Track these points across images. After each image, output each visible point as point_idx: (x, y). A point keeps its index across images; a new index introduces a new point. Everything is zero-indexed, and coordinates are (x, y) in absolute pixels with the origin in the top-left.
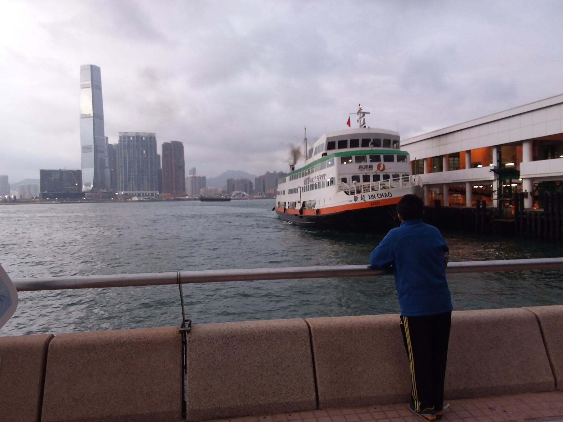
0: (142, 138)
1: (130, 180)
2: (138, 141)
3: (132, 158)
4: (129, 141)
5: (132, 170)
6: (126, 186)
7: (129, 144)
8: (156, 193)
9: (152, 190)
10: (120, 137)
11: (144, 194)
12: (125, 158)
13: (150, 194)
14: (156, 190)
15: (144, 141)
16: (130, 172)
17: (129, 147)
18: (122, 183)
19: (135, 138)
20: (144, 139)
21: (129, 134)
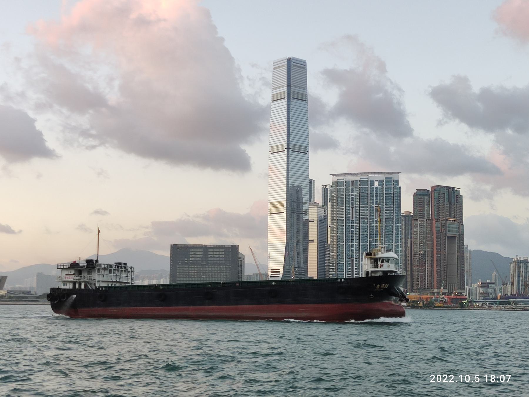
0: (372, 183)
2: (364, 189)
3: (352, 222)
15: (376, 188)
20: (376, 184)
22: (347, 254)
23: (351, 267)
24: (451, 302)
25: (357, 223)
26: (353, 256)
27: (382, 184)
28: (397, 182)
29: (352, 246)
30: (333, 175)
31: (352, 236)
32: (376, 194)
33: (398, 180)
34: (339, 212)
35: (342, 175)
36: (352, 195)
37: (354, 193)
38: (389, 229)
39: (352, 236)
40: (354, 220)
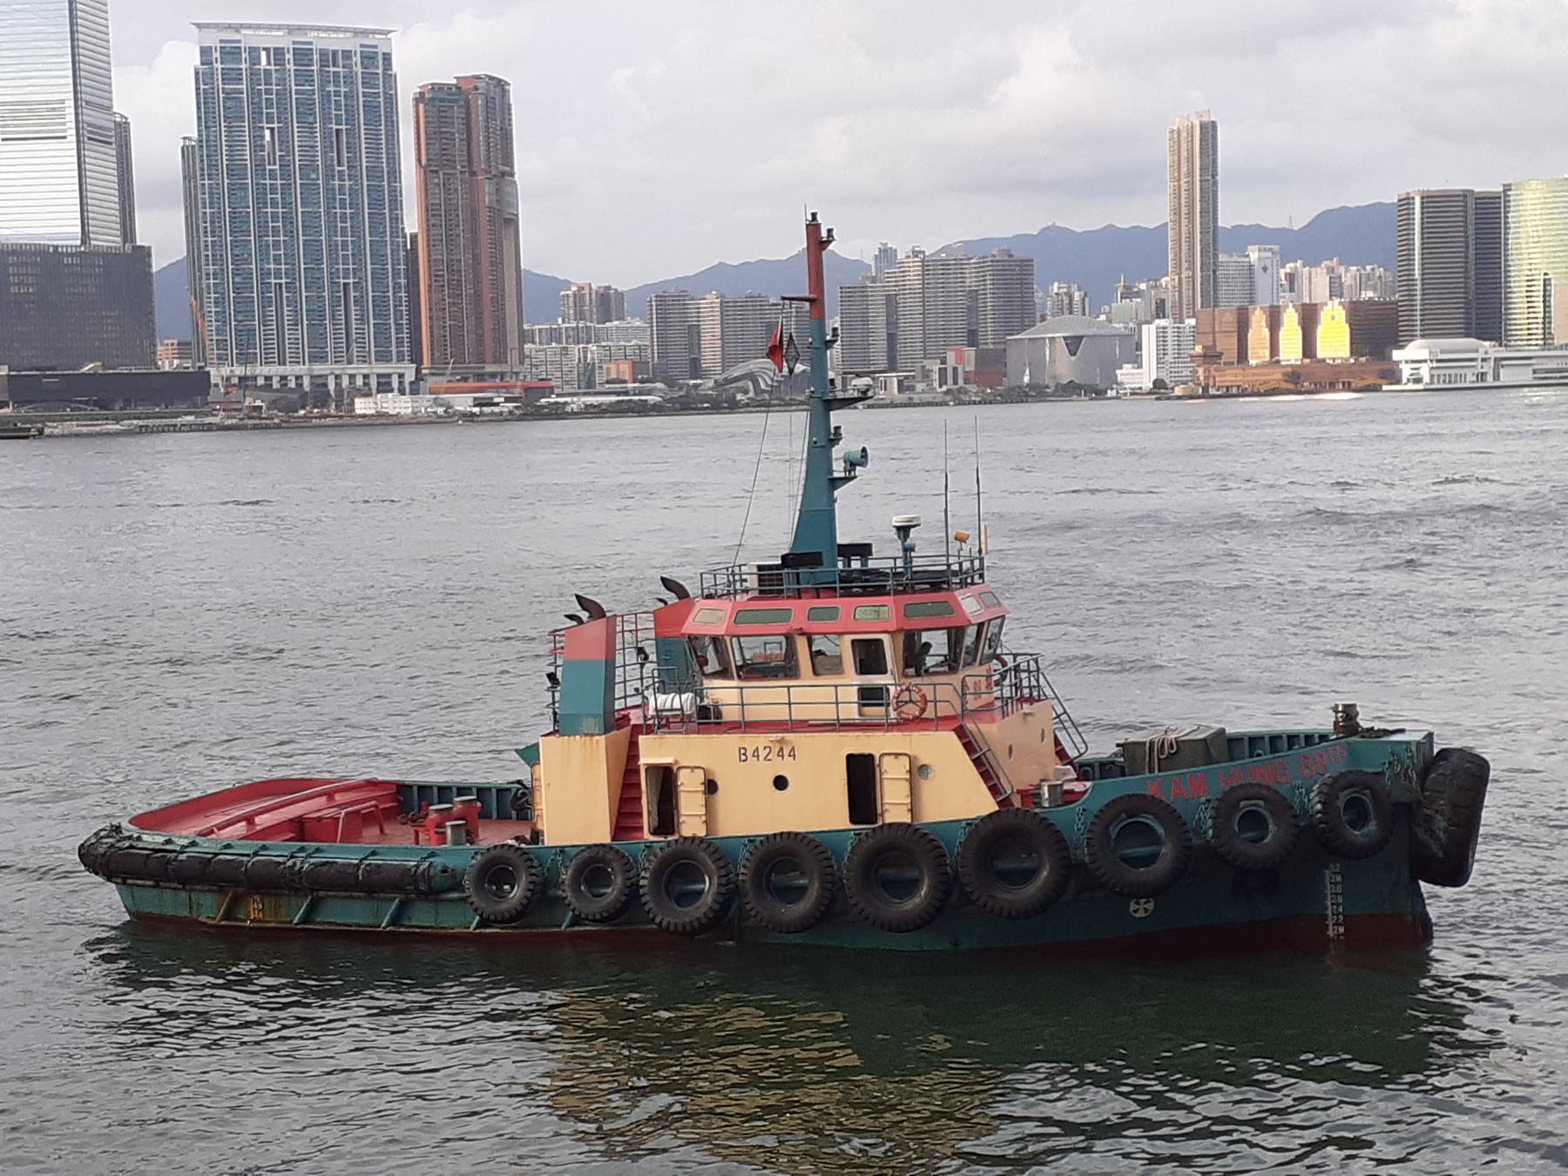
1: (266, 301)
2: (304, 77)
3: (272, 174)
4: (254, 74)
5: (276, 245)
6: (245, 337)
7: (254, 94)
8: (401, 376)
9: (383, 357)
10: (205, 52)
11: (345, 382)
12: (236, 170)
13: (374, 384)
14: (400, 359)
16: (263, 249)
17: (256, 115)
18: (222, 316)
19: (289, 56)
21: (248, 39)
22: (261, 269)
23: (274, 308)
24: (1382, 378)
25: (214, 177)
26: (278, 275)
27: (349, 62)
28: (387, 58)
29: (276, 245)
30: (198, 26)
31: (275, 218)
32: (337, 93)
33: (390, 54)
34: (230, 146)
35: (229, 27)
36: (268, 92)
37: (343, 89)
38: (375, 197)
39: (275, 218)
40: (277, 167)
